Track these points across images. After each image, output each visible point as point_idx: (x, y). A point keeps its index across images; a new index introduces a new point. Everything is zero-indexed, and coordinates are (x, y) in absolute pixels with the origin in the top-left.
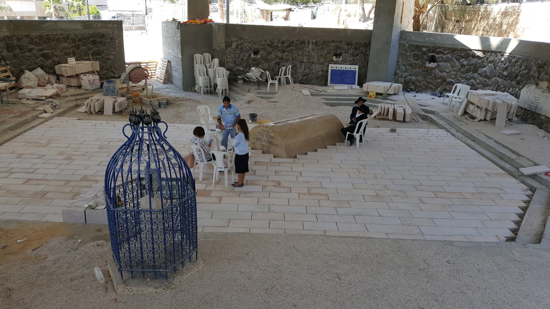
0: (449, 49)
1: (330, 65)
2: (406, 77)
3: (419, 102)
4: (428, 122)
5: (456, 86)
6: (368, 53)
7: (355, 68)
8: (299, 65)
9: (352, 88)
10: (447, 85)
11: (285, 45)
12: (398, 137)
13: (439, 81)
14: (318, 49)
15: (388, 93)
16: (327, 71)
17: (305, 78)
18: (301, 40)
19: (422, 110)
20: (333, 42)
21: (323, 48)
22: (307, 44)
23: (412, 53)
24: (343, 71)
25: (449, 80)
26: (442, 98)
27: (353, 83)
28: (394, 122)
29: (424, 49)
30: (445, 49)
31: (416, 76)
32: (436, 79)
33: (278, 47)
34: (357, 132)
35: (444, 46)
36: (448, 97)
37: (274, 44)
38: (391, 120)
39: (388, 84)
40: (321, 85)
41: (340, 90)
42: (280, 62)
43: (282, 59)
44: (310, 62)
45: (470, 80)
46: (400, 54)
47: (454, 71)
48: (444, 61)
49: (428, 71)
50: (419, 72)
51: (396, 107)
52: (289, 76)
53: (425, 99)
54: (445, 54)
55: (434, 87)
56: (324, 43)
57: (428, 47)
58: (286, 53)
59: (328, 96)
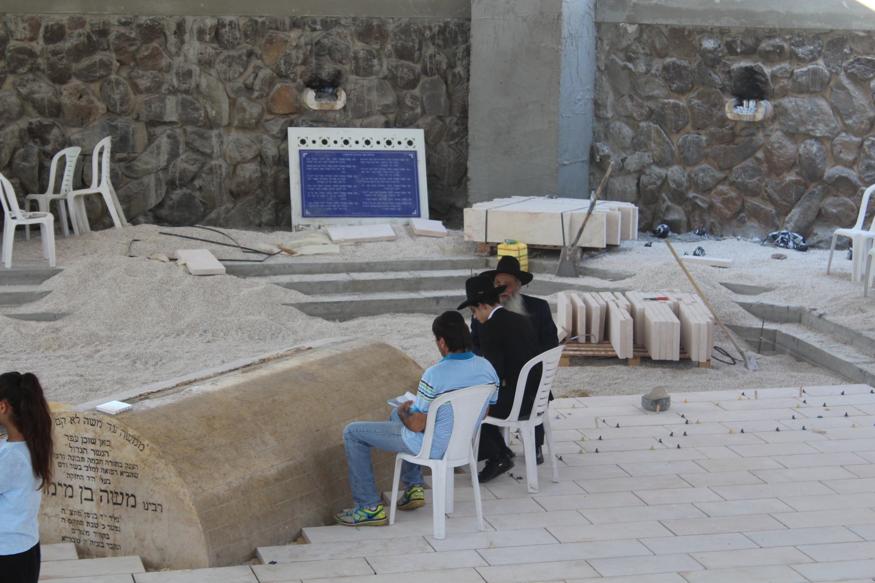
0: (817, 36)
1: (295, 134)
2: (640, 172)
3: (726, 276)
4: (785, 358)
6: (459, 69)
7: (412, 139)
8: (140, 134)
9: (412, 233)
10: (826, 193)
11: (67, 45)
12: (688, 429)
13: (791, 177)
14: (230, 61)
15: (584, 242)
16: (282, 161)
17: (177, 194)
18: (143, 20)
19: (748, 307)
20: (295, 24)
21: (250, 54)
22: (172, 39)
23: (657, 65)
24: (357, 156)
25: (832, 171)
26: (816, 258)
27: (410, 210)
28: (642, 370)
29: (709, 44)
30: (801, 37)
31: (685, 162)
32: (775, 169)
33: (32, 54)
34: (525, 413)
35: (796, 24)
36: (846, 244)
37: (12, 44)
38: (625, 362)
39: (576, 207)
40: (260, 227)
41: (358, 243)
42: (48, 128)
43: (56, 110)
44: (194, 122)
46: (606, 71)
47: (848, 129)
48: (801, 90)
49: (738, 140)
50: (698, 144)
51: (637, 299)
52: (104, 188)
53: (742, 258)
54: (801, 61)
55: (770, 208)
56: (255, 30)
57: (723, 32)
58: (75, 82)
59: (310, 270)
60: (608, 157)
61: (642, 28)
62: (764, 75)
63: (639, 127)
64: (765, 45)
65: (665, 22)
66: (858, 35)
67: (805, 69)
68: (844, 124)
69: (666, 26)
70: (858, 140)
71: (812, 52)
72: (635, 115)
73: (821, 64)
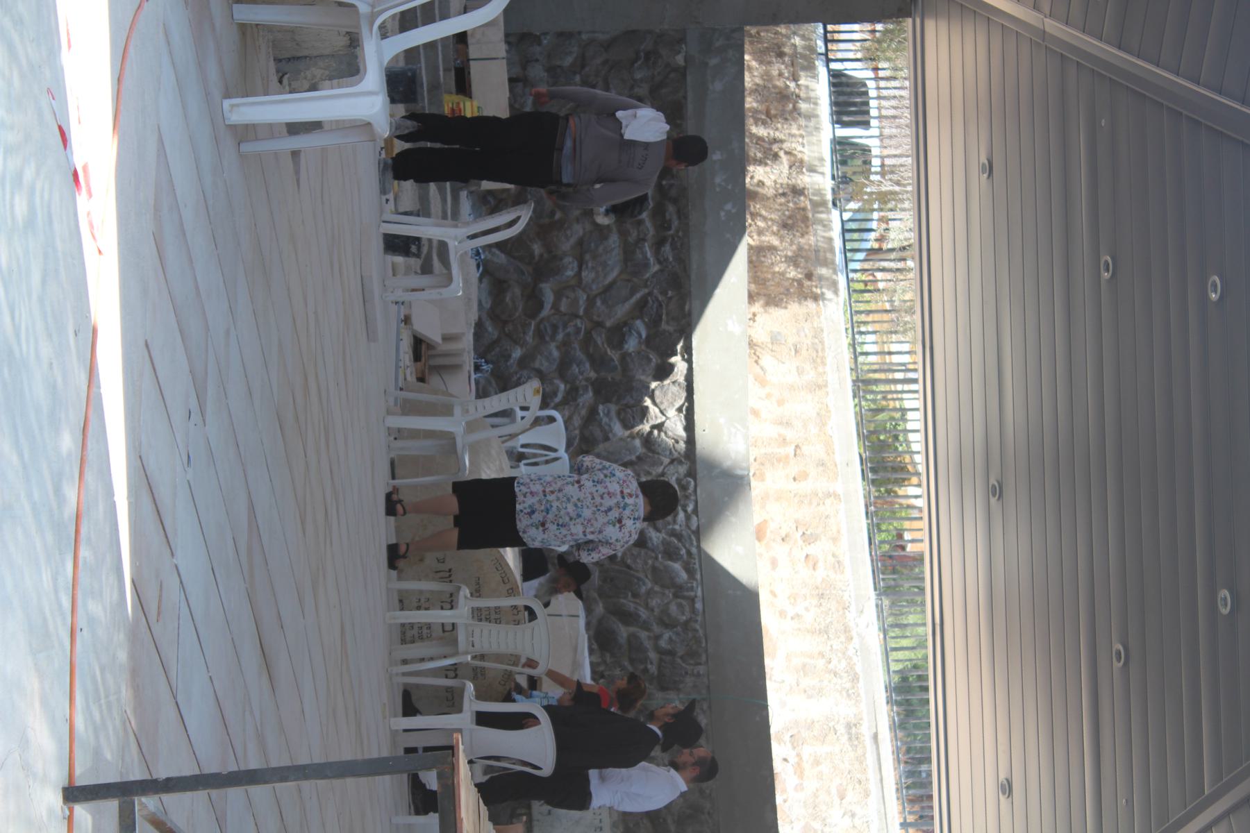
0: (683, 261)
5: (552, 420)
13: (537, 249)
25: (548, 292)
45: (562, 376)
47: (591, 302)
48: (628, 253)
60: (540, 44)
61: (682, 72)
62: (640, 213)
63: (575, 73)
64: (671, 209)
65: (689, 99)
66: (684, 304)
67: (649, 254)
68: (596, 296)
69: (685, 97)
70: (581, 312)
71: (666, 260)
72: (587, 69)
73: (656, 268)
